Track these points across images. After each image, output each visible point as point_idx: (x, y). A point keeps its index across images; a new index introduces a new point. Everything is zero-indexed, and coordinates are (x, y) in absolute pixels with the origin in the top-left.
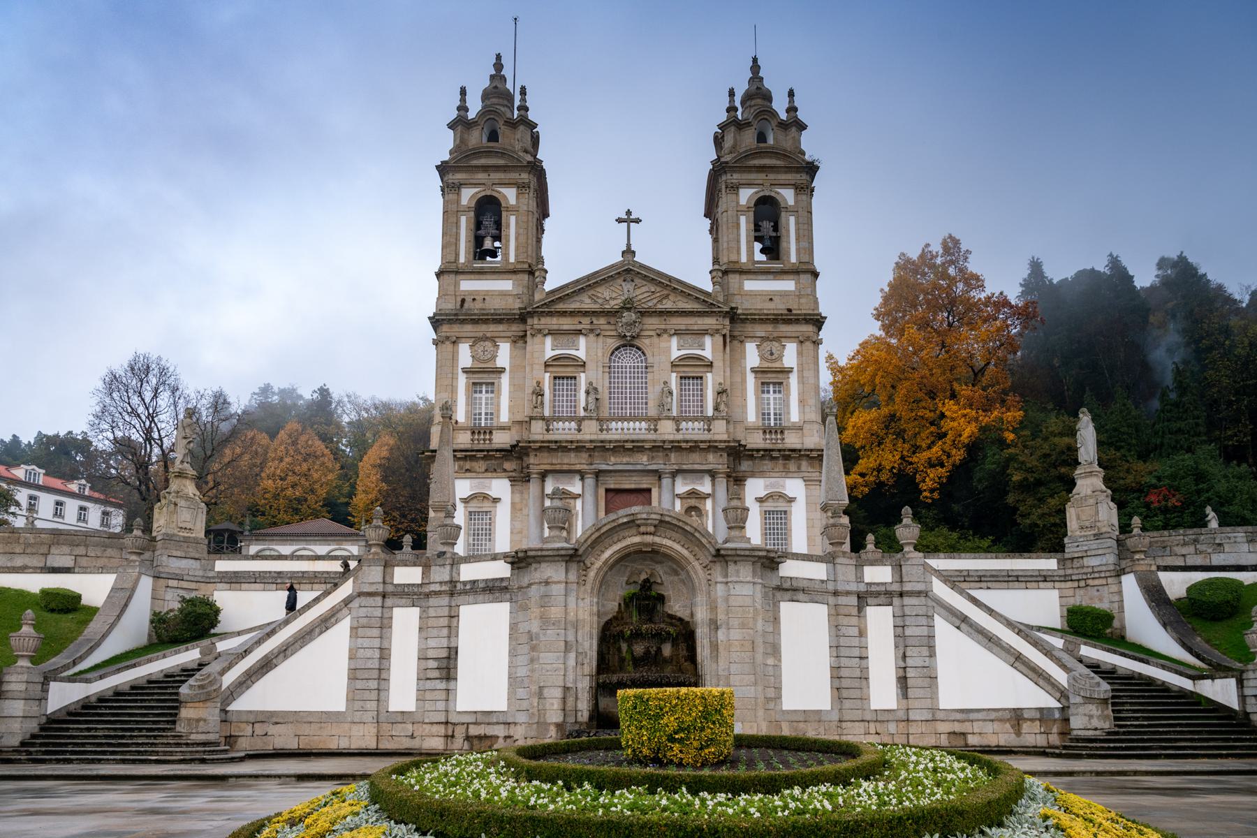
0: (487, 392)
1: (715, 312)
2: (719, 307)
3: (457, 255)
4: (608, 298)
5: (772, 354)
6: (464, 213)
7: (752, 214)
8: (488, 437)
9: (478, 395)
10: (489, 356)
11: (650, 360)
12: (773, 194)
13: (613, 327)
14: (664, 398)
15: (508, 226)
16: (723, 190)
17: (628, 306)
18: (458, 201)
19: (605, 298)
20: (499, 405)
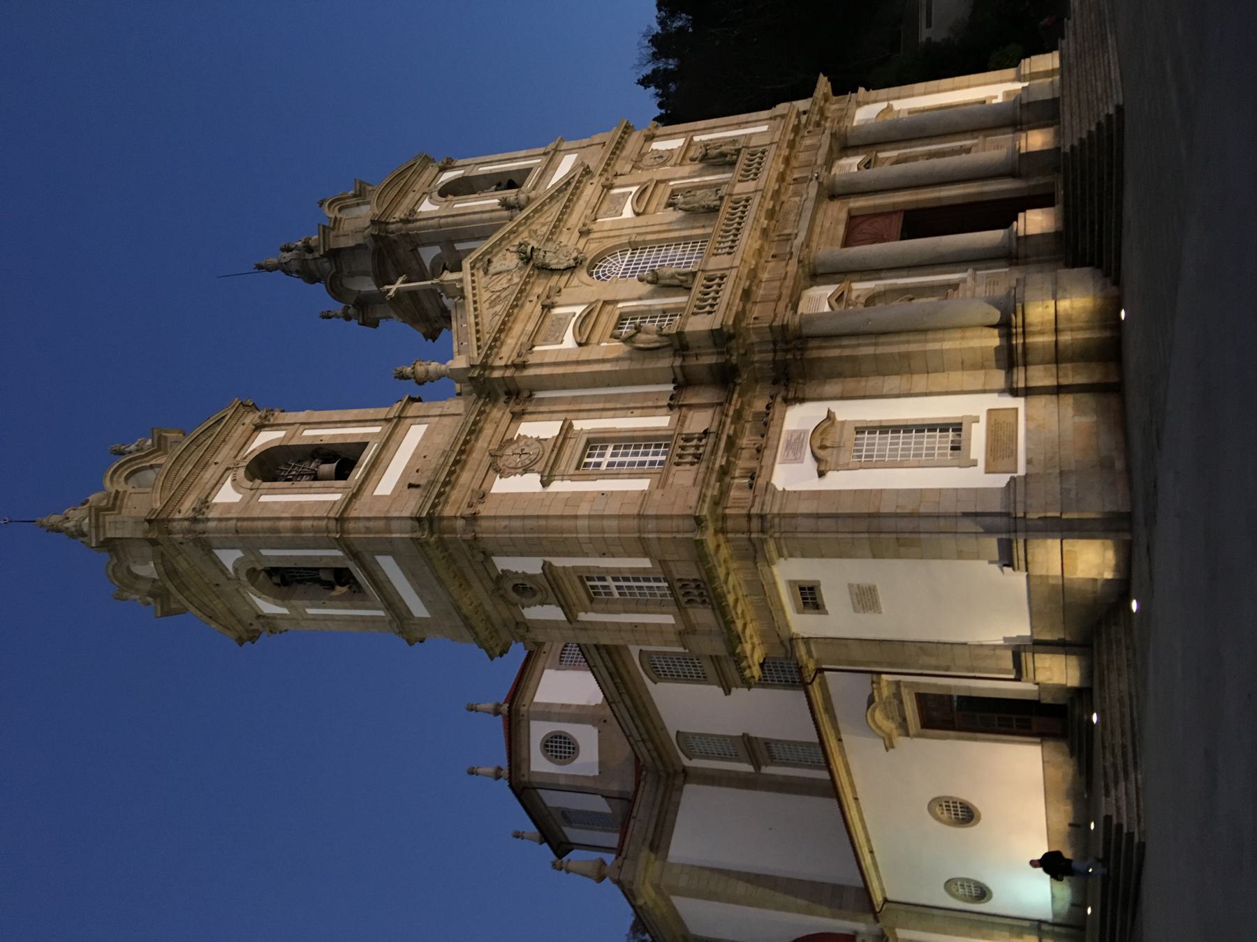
0: (602, 455)
1: (579, 182)
2: (573, 177)
3: (324, 502)
4: (505, 286)
5: (661, 157)
6: (256, 497)
7: (456, 198)
8: (695, 442)
9: (604, 467)
10: (537, 445)
11: (625, 240)
12: (441, 185)
13: (556, 278)
14: (696, 199)
15: (316, 436)
16: (411, 225)
17: (527, 258)
18: (229, 506)
19: (505, 289)
20: (634, 430)
